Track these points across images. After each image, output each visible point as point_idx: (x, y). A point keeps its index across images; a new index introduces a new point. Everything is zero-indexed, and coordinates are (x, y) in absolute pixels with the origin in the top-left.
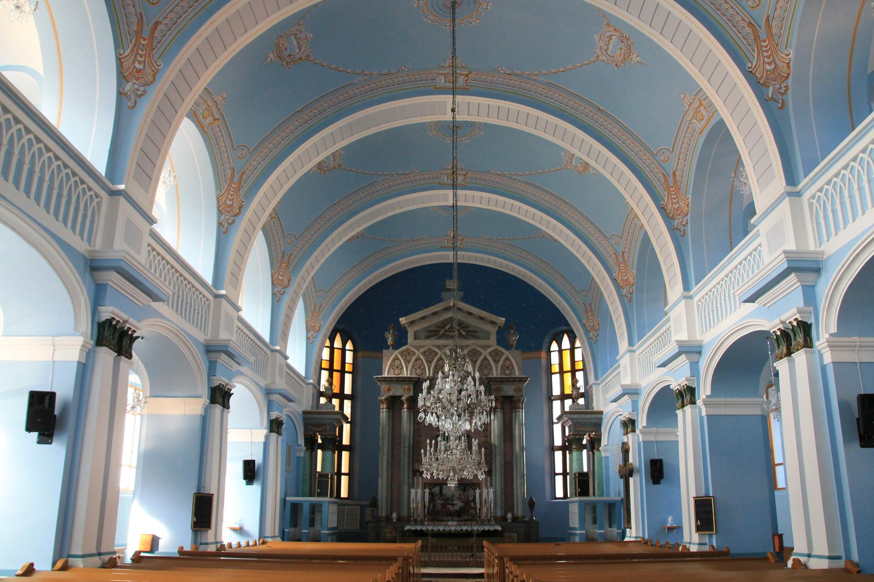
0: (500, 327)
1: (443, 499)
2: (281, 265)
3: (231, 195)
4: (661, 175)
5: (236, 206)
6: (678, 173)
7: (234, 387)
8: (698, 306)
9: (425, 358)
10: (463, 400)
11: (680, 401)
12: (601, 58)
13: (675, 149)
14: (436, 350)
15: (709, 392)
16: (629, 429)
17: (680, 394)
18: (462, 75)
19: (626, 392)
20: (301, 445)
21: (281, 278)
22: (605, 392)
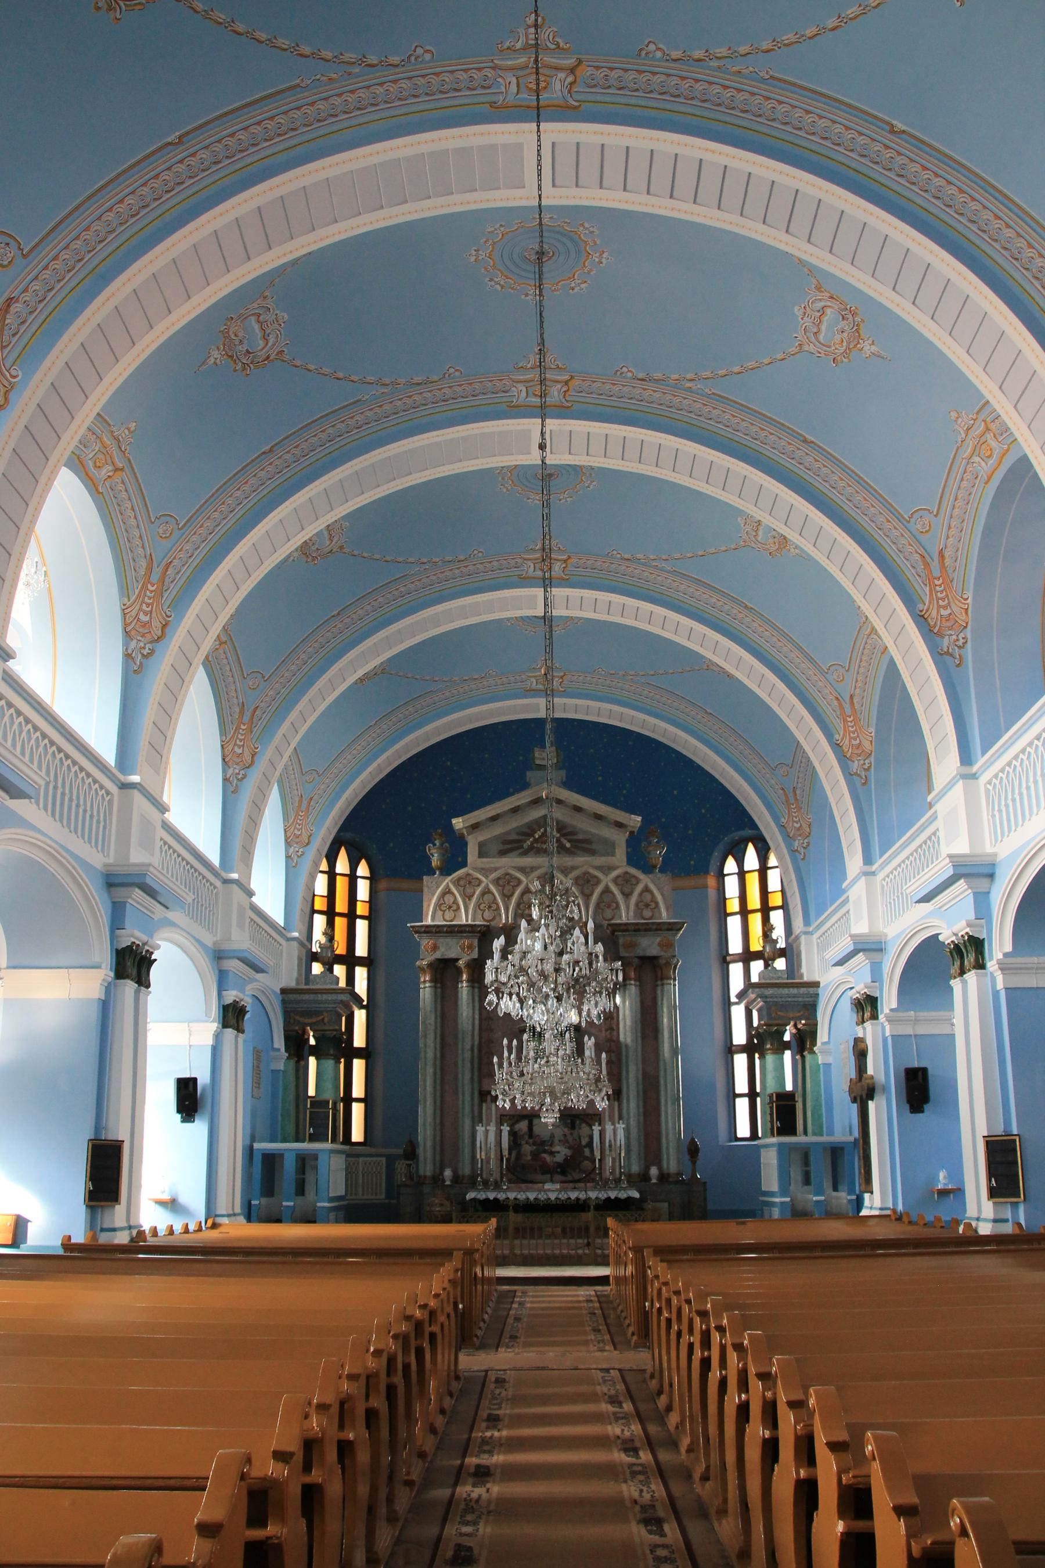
0: (632, 833)
1: (534, 1144)
2: (238, 728)
3: (148, 605)
4: (917, 557)
5: (156, 625)
6: (947, 554)
7: (158, 947)
8: (987, 791)
10: (565, 970)
11: (957, 963)
12: (806, 348)
13: (942, 512)
14: (519, 875)
15: (1008, 948)
16: (867, 1015)
17: (957, 951)
18: (557, 382)
19: (860, 947)
20: (278, 1050)
21: (239, 751)
22: (823, 947)
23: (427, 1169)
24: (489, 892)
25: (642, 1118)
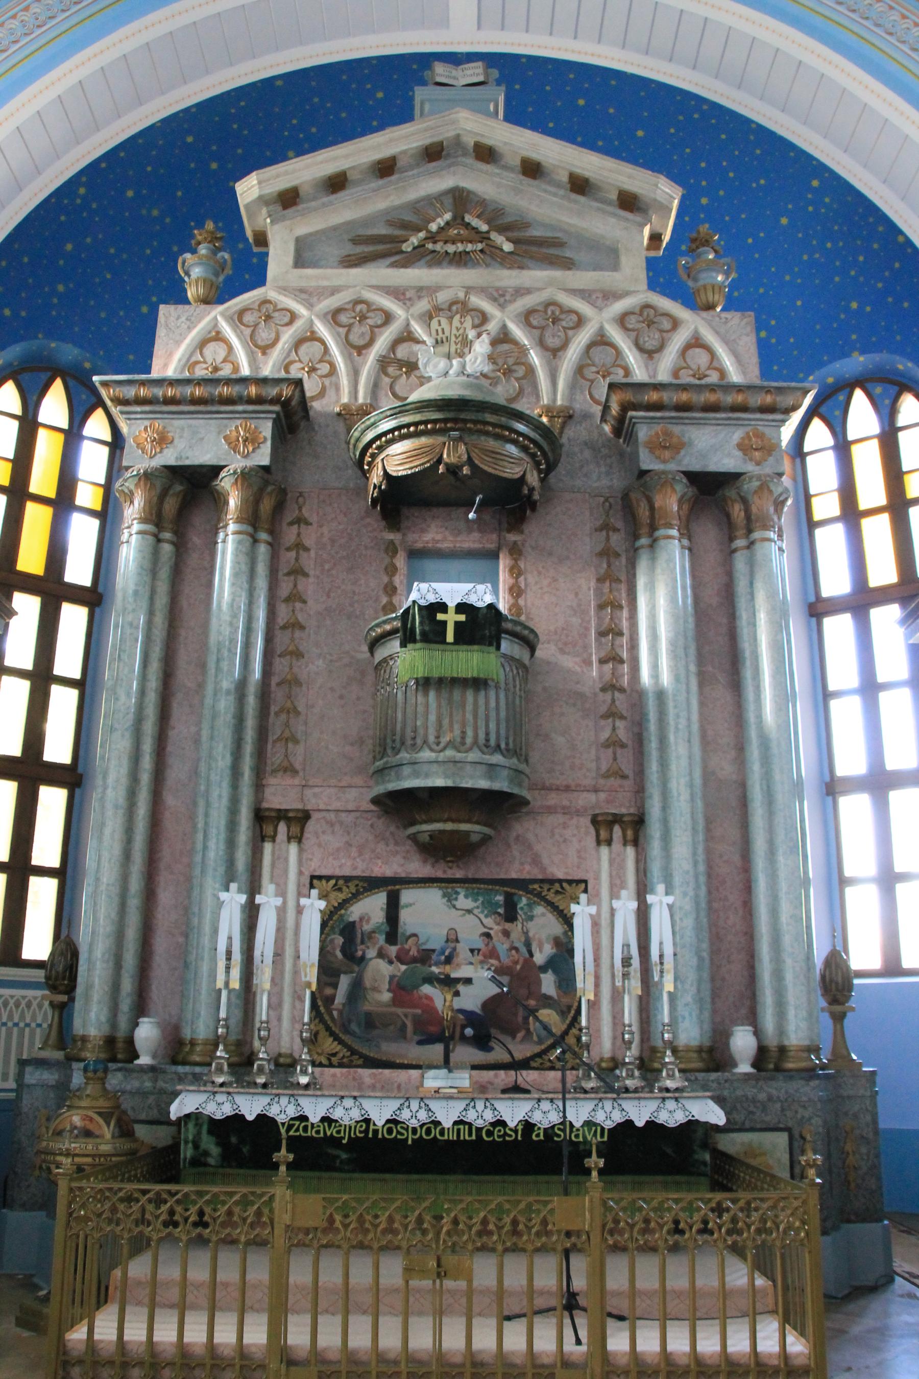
1: (400, 959)
9: (336, 336)
24: (313, 337)
25: (703, 890)
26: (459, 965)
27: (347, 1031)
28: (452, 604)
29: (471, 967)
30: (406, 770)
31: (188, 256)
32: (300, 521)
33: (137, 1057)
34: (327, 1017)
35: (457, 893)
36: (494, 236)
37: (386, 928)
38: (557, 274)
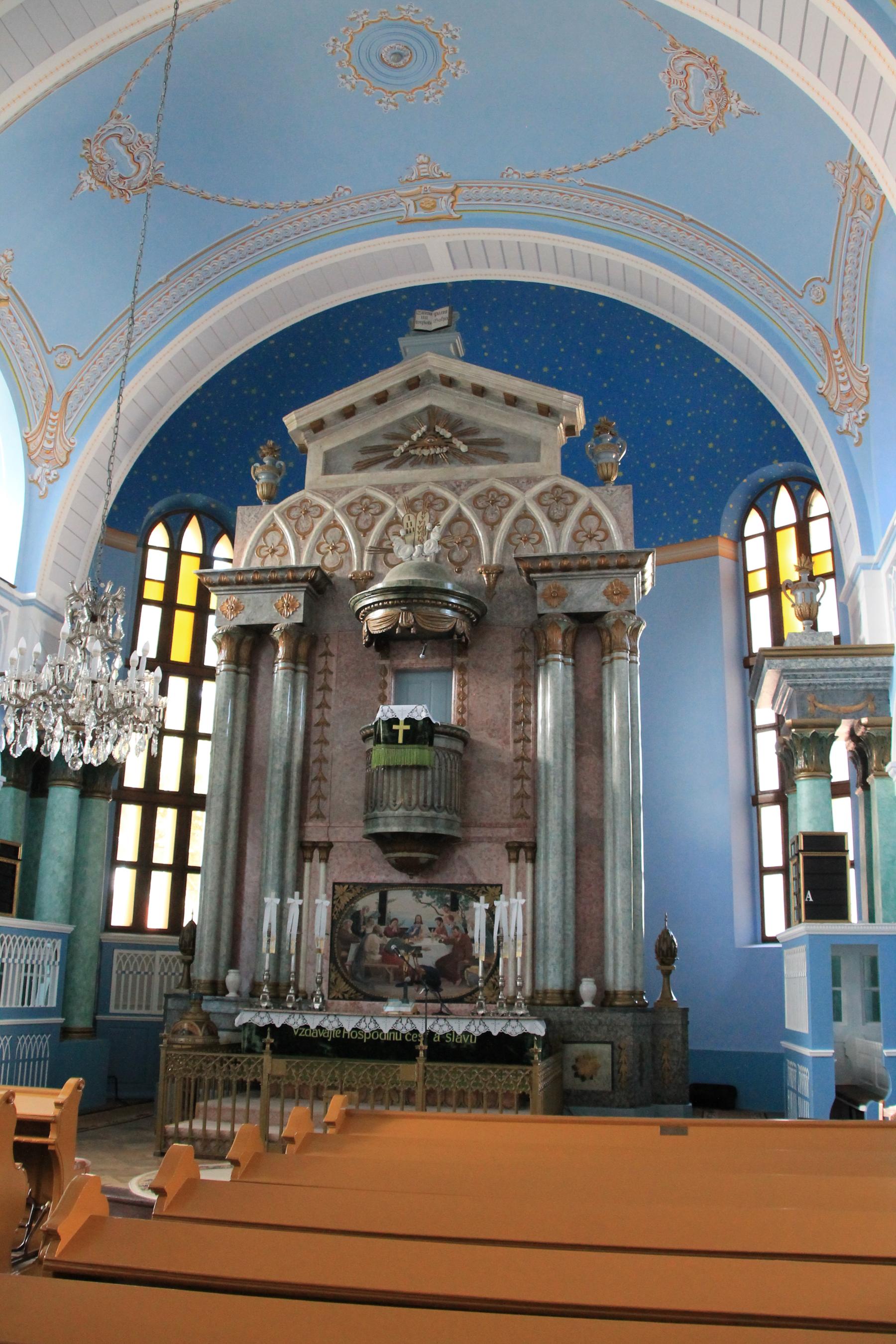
1: (387, 934)
9: (349, 523)
23: (202, 971)
24: (335, 525)
26: (422, 938)
27: (354, 979)
28: (402, 719)
29: (429, 939)
30: (380, 821)
31: (257, 465)
32: (327, 654)
33: (228, 992)
34: (342, 970)
35: (422, 893)
36: (454, 440)
37: (378, 915)
38: (496, 467)
